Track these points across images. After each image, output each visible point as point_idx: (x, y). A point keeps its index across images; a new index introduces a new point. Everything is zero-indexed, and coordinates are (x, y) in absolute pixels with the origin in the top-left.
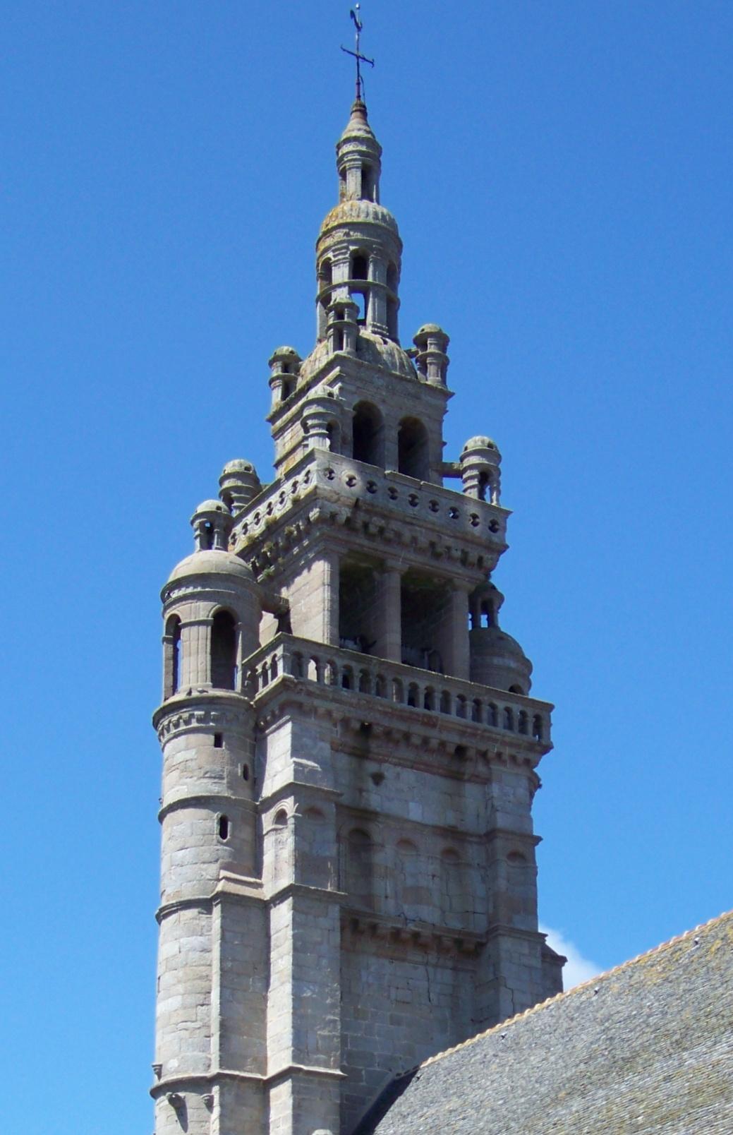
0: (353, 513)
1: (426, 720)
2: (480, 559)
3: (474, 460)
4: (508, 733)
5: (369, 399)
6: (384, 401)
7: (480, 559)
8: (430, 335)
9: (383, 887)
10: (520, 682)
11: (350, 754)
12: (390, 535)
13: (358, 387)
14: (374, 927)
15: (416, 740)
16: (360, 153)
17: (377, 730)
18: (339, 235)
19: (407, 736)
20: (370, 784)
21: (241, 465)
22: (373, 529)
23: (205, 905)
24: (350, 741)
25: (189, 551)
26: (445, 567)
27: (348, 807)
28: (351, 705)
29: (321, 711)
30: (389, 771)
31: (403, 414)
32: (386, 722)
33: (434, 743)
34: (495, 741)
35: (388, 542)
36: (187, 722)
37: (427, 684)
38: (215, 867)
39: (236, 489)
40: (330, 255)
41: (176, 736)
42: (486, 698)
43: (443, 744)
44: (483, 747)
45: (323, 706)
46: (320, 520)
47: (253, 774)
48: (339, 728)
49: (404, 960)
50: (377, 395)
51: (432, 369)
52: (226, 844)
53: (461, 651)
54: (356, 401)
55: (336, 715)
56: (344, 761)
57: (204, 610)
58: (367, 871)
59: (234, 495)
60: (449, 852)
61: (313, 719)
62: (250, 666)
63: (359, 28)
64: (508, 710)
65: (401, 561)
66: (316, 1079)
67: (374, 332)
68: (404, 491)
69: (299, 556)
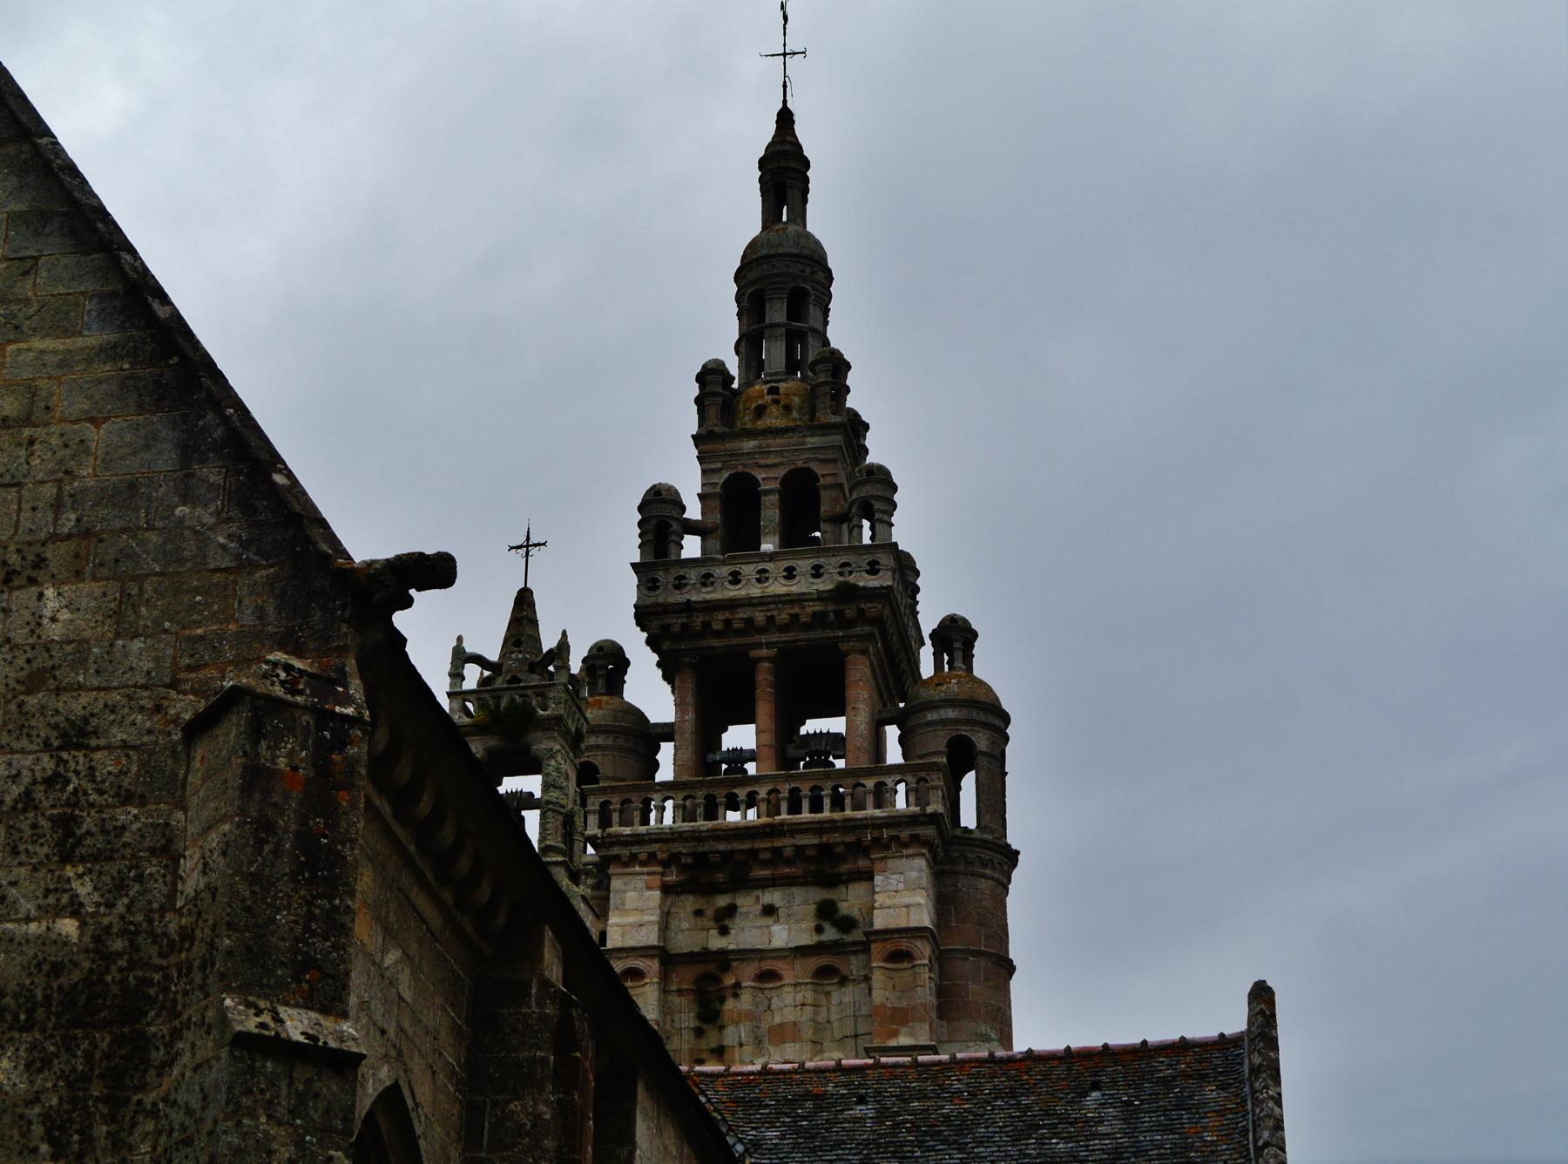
1: (767, 830)
4: (878, 813)
10: (964, 731)
12: (737, 625)
13: (724, 462)
19: (753, 853)
22: (716, 626)
29: (643, 856)
31: (781, 472)
32: (722, 847)
34: (866, 827)
35: (740, 633)
43: (800, 850)
44: (850, 838)
45: (642, 851)
54: (726, 475)
55: (660, 856)
61: (637, 868)
68: (749, 570)
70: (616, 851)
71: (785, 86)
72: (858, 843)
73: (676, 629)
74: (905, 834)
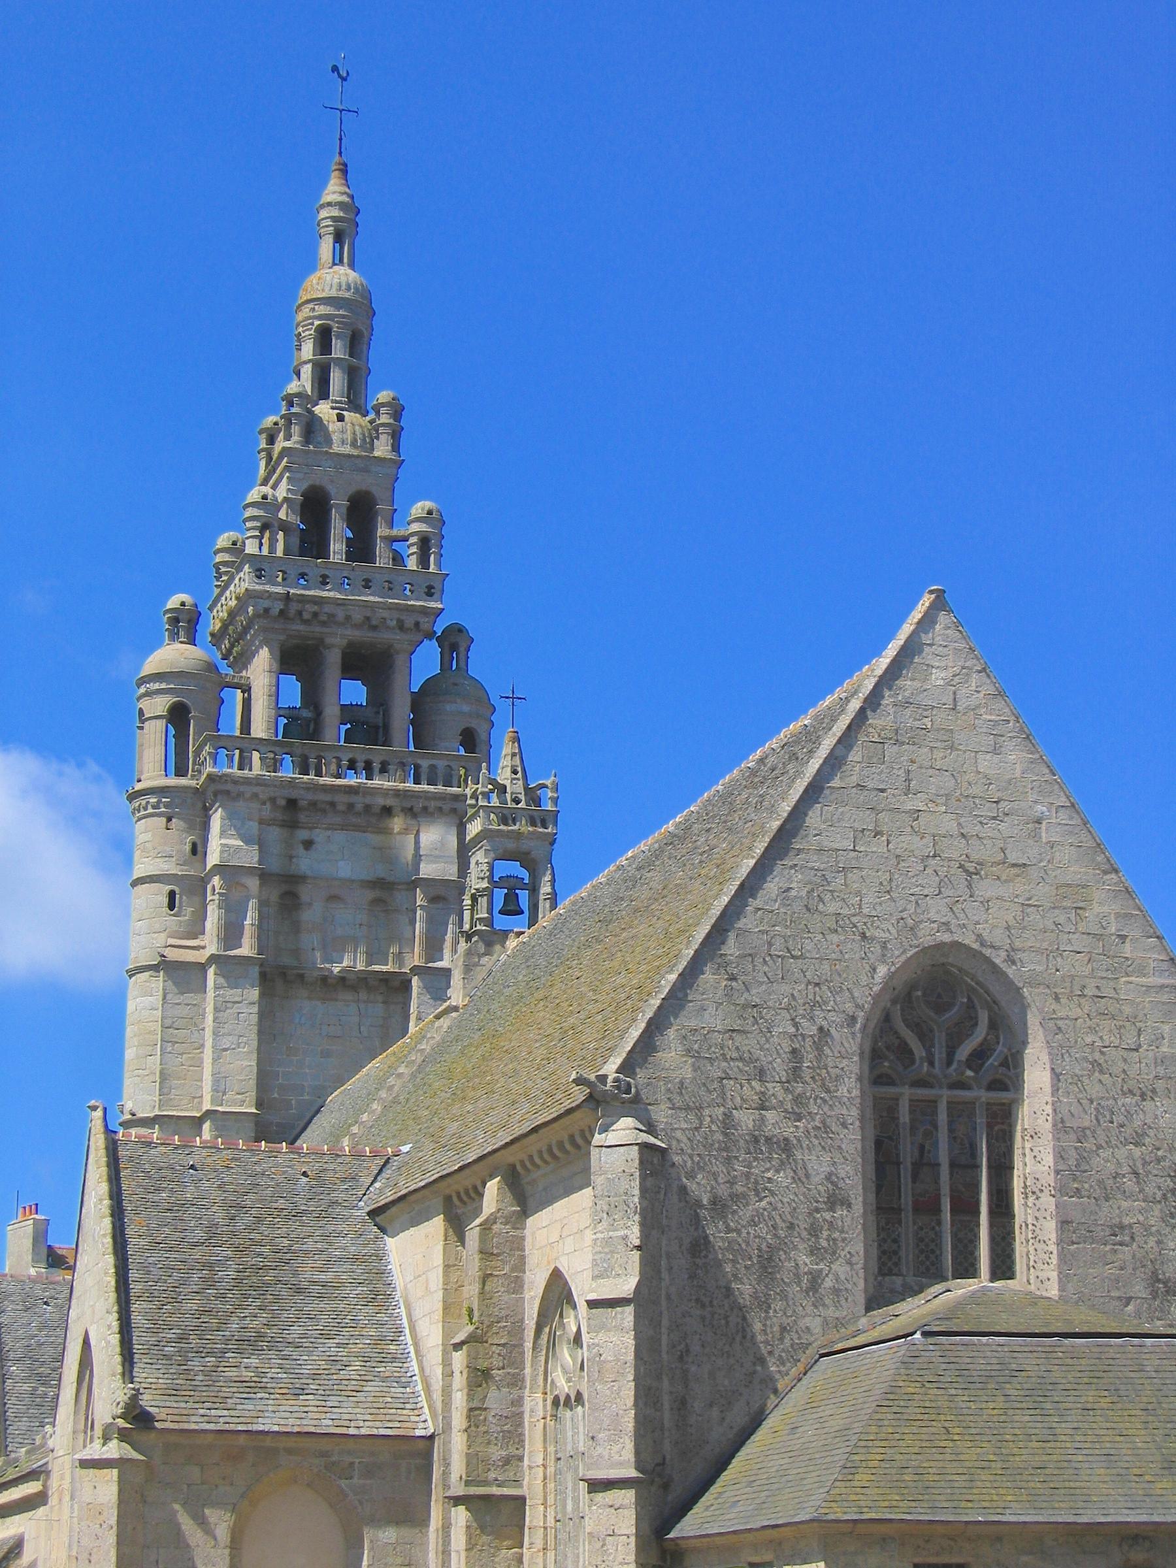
0: (286, 605)
2: (417, 624)
3: (415, 527)
4: (431, 788)
5: (317, 483)
6: (332, 481)
7: (417, 624)
8: (383, 405)
9: (311, 939)
10: (473, 724)
11: (282, 826)
12: (324, 618)
14: (301, 976)
15: (341, 808)
16: (334, 219)
17: (303, 803)
18: (306, 311)
20: (301, 850)
21: (228, 538)
22: (306, 616)
23: (154, 968)
24: (279, 816)
25: (158, 644)
26: (385, 636)
27: (278, 875)
28: (275, 786)
29: (248, 795)
30: (319, 836)
31: (352, 490)
32: (310, 796)
33: (359, 807)
35: (324, 624)
36: (145, 809)
37: (351, 756)
38: (163, 935)
39: (225, 564)
40: (301, 329)
41: (140, 819)
42: (410, 760)
45: (248, 790)
46: (256, 615)
47: (198, 850)
48: (268, 806)
49: (336, 1000)
50: (323, 475)
51: (383, 438)
52: (174, 915)
53: (401, 713)
54: (305, 486)
56: (275, 834)
57: (159, 705)
58: (296, 928)
59: (223, 569)
60: (377, 901)
62: (197, 753)
63: (344, 79)
64: (433, 768)
65: (337, 640)
66: (233, 1117)
67: (333, 408)
69: (252, 641)
70: (229, 787)
71: (341, 139)
72: (411, 809)
73: (275, 611)
74: (447, 807)
